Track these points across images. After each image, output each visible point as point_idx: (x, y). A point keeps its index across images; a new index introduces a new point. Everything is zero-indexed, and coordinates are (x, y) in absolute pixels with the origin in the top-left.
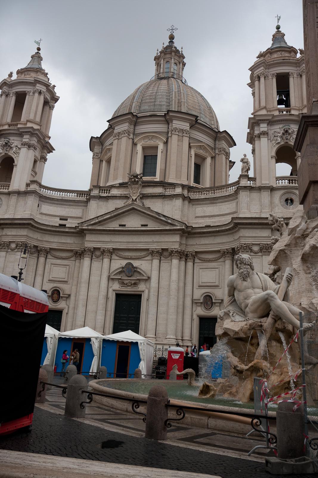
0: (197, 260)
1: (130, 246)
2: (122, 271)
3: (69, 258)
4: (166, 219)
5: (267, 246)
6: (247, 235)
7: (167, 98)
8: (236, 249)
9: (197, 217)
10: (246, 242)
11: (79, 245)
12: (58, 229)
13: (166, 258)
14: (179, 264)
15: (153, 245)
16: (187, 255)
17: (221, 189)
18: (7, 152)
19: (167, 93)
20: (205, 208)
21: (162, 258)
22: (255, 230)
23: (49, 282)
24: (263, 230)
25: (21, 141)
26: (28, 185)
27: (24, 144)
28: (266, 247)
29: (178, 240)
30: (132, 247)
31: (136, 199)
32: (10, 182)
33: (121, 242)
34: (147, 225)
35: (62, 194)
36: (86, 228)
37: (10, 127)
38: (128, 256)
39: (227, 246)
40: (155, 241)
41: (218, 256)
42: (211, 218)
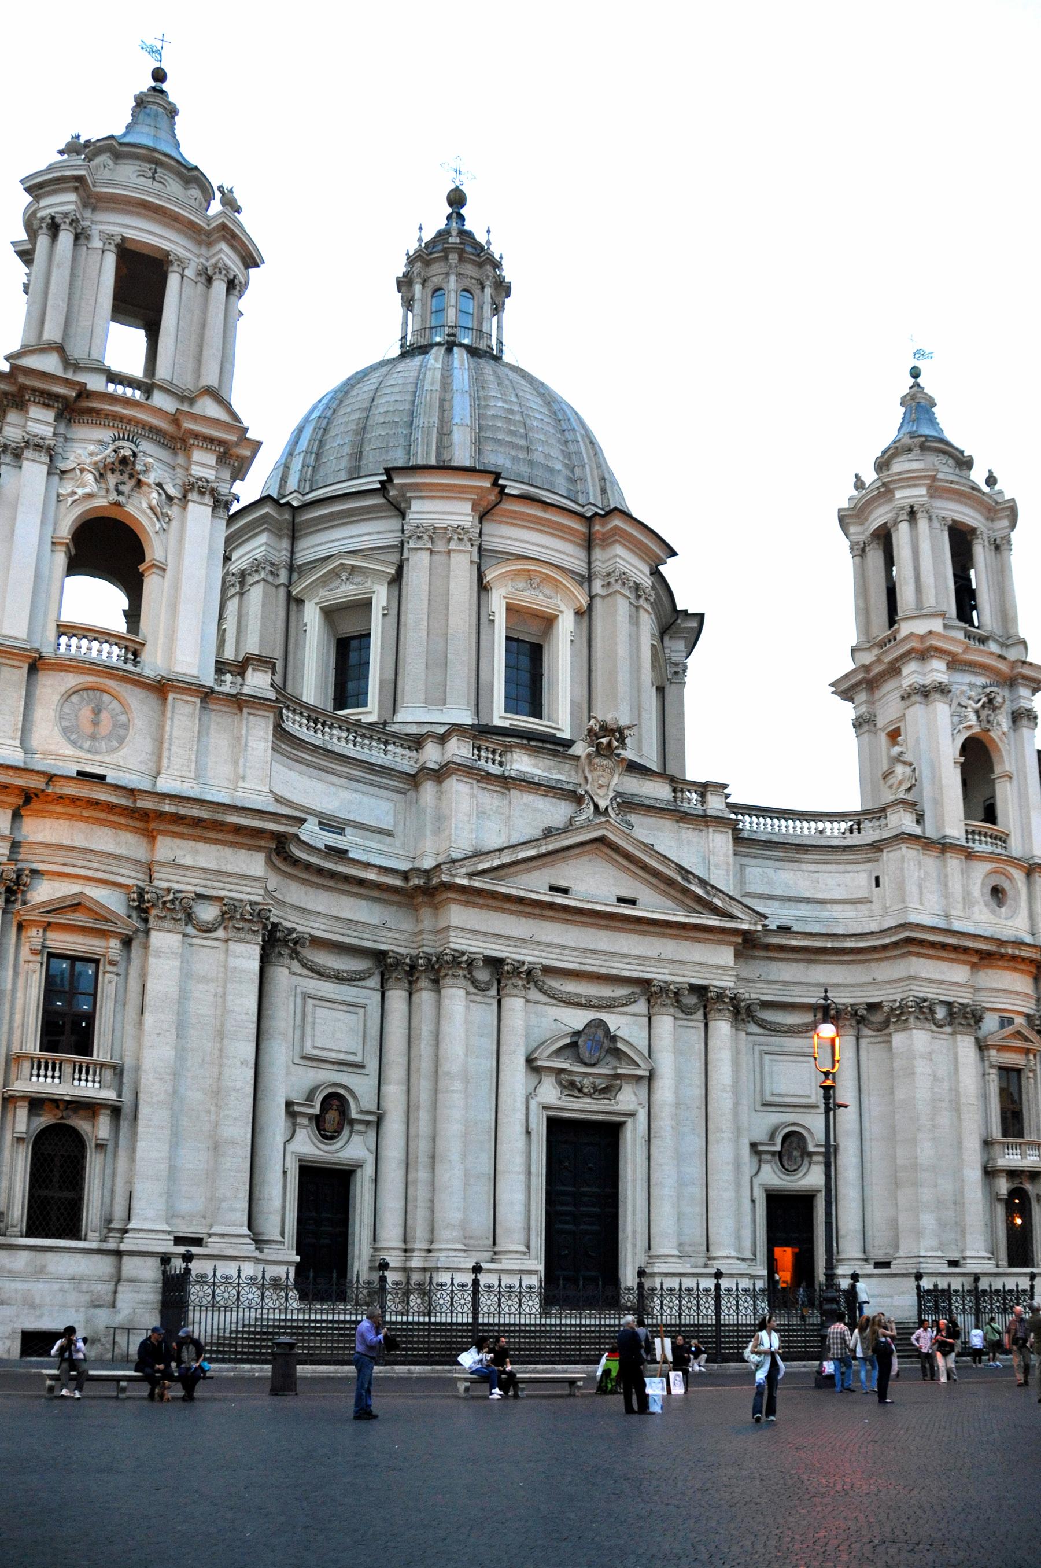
1: (591, 965)
2: (572, 1048)
3: (359, 980)
4: (707, 893)
6: (923, 975)
7: (563, 451)
8: (886, 1009)
10: (929, 996)
11: (403, 937)
13: (691, 1014)
15: (660, 970)
23: (302, 1062)
24: (955, 965)
29: (731, 963)
30: (595, 969)
31: (607, 808)
33: (562, 947)
34: (632, 902)
36: (465, 882)
38: (579, 996)
39: (848, 995)
40: (662, 956)
42: (787, 904)
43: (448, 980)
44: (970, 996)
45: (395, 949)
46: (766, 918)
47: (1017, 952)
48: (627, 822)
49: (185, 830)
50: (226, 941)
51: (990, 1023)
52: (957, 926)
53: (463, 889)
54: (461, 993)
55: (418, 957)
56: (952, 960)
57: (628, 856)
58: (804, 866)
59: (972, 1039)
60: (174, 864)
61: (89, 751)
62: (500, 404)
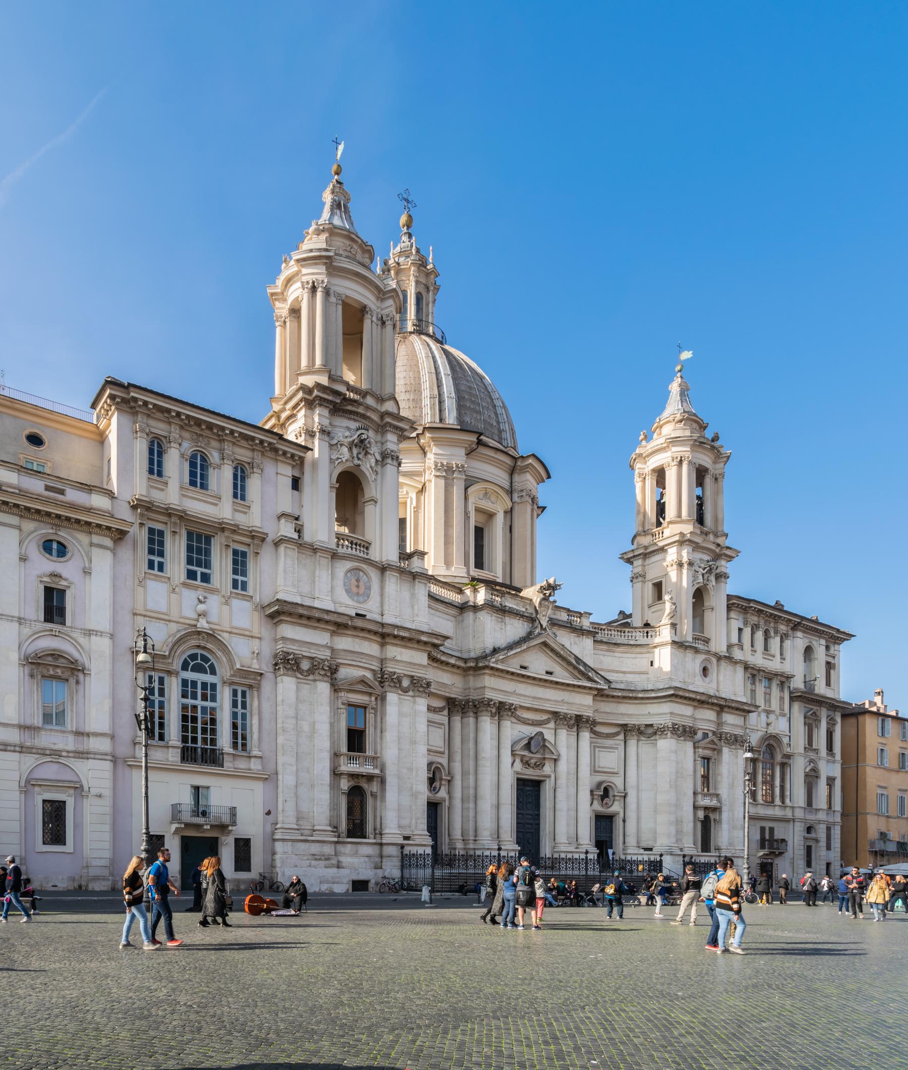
4: (586, 670)
29: (591, 704)
38: (529, 720)
43: (482, 714)
45: (460, 698)
46: (611, 682)
48: (554, 634)
49: (399, 642)
50: (413, 697)
51: (699, 735)
52: (691, 688)
53: (492, 668)
54: (488, 719)
55: (468, 702)
57: (552, 650)
58: (616, 654)
60: (394, 659)
61: (356, 602)
62: (465, 383)
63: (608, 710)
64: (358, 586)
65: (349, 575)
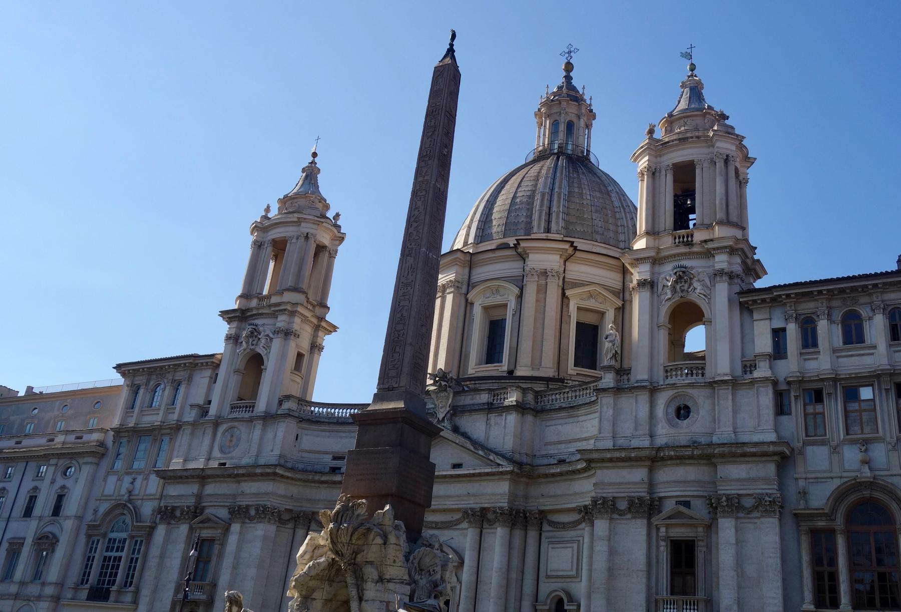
0: (546, 527)
4: (485, 454)
5: (637, 501)
7: (528, 209)
9: (547, 444)
12: (324, 478)
14: (511, 535)
16: (526, 518)
17: (587, 389)
18: (253, 347)
19: (529, 197)
20: (560, 427)
21: (485, 525)
22: (619, 470)
25: (275, 325)
26: (280, 403)
27: (274, 333)
28: (637, 504)
31: (444, 418)
32: (256, 400)
35: (338, 413)
37: (260, 301)
41: (577, 519)
42: (569, 445)
44: (644, 490)
47: (672, 453)
51: (669, 506)
52: (635, 443)
56: (632, 467)
59: (645, 521)
63: (559, 492)
64: (231, 441)
65: (226, 434)
